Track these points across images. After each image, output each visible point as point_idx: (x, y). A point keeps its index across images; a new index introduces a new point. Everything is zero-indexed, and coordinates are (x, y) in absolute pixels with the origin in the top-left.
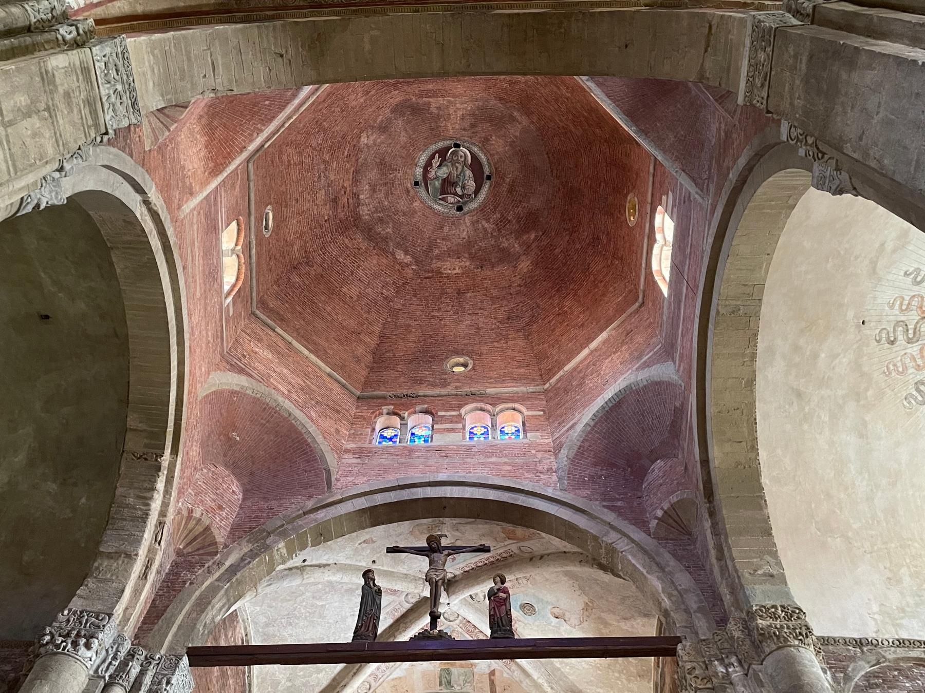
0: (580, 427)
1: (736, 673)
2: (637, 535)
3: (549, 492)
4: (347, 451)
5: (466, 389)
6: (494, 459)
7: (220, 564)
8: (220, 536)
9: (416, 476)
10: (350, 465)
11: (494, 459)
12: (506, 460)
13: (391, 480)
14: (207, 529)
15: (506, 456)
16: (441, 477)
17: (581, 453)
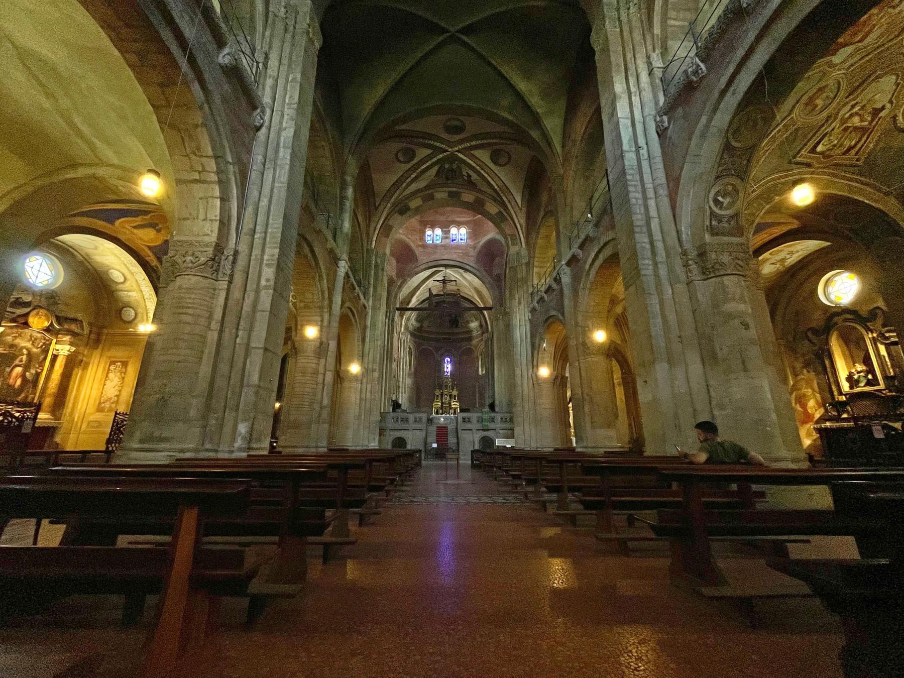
0: (481, 244)
1: (501, 317)
2: (489, 279)
3: (471, 264)
4: (420, 246)
5: (450, 219)
6: (458, 251)
7: (396, 285)
8: (395, 277)
9: (437, 257)
10: (422, 252)
11: (458, 251)
12: (461, 251)
13: (433, 258)
14: (392, 277)
15: (462, 250)
16: (445, 258)
17: (480, 252)
